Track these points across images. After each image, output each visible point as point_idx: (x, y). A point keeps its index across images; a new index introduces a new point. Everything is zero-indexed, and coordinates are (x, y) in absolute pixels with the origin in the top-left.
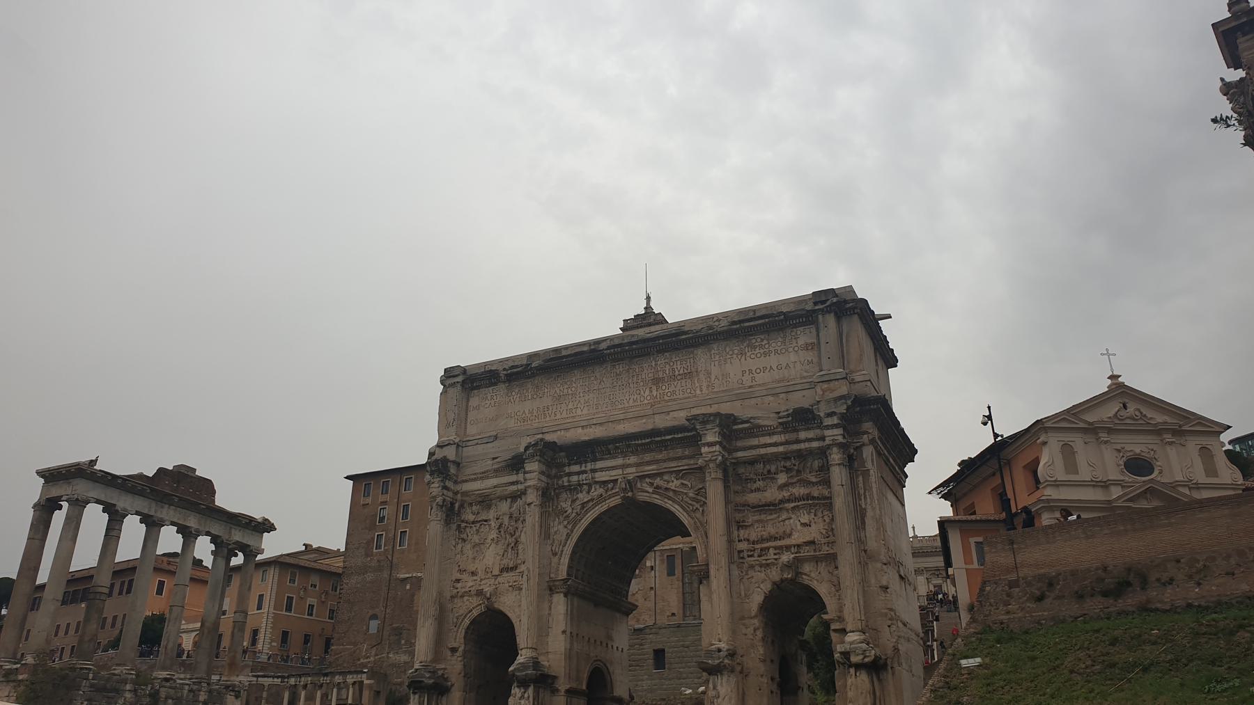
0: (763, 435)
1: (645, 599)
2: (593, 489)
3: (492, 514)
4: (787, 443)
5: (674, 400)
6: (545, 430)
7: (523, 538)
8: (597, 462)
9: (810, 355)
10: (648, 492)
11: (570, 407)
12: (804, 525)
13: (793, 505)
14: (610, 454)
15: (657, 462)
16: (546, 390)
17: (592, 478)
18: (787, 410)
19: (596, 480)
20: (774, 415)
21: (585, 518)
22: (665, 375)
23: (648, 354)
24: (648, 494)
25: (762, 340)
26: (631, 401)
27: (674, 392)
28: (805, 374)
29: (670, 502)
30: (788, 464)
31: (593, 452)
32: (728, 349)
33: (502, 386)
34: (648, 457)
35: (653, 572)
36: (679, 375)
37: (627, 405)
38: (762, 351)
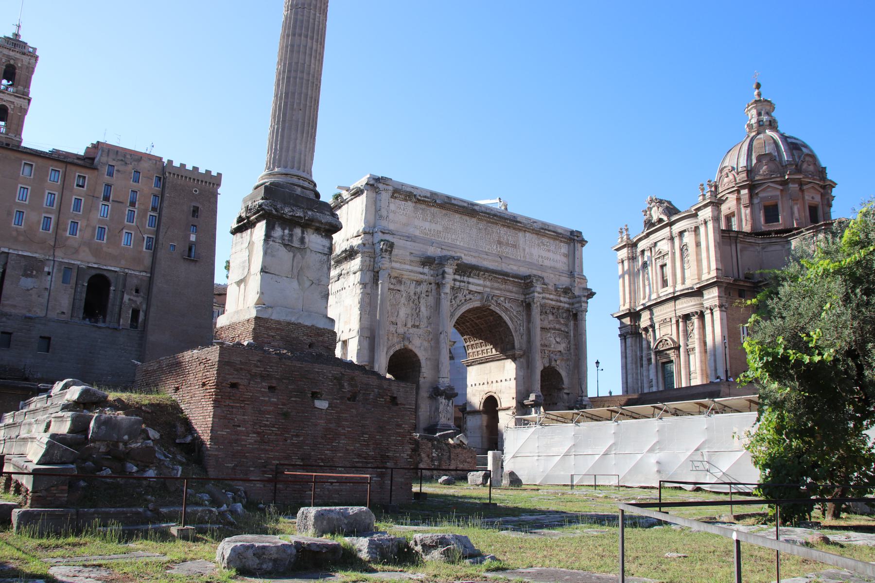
0: (547, 293)
1: (39, 296)
3: (402, 288)
5: (509, 258)
6: (443, 247)
7: (423, 309)
9: (565, 260)
15: (500, 290)
26: (487, 249)
27: (508, 253)
30: (554, 311)
31: (470, 273)
33: (409, 203)
34: (496, 285)
35: (49, 277)
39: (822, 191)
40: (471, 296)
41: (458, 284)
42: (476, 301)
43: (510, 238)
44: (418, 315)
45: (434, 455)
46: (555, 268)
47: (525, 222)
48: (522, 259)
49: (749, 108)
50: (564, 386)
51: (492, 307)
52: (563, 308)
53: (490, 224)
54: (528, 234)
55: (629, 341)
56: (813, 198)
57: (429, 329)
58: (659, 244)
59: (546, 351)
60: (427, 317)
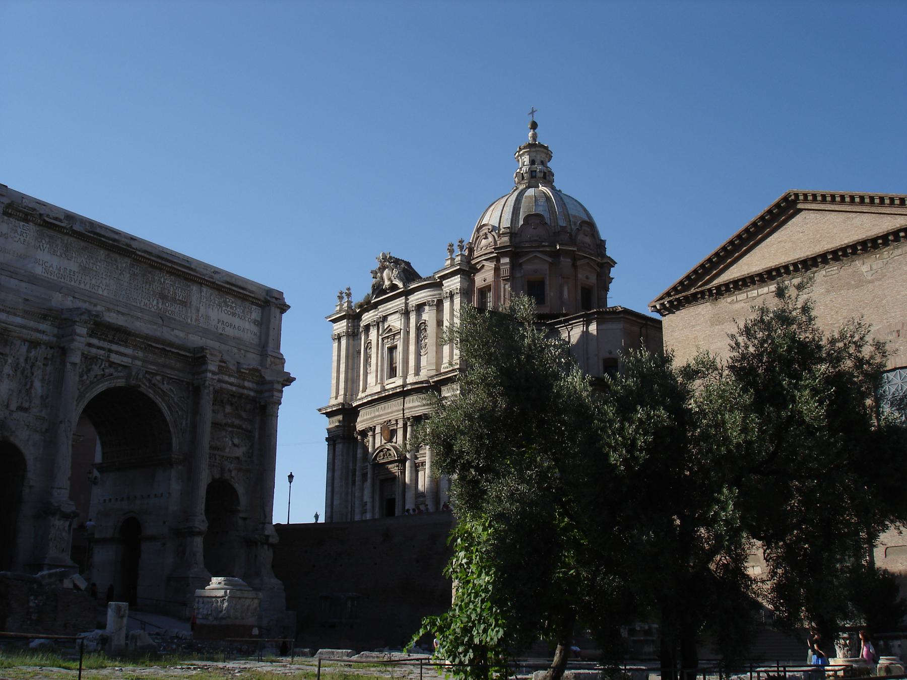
0: (226, 375)
2: (103, 366)
4: (239, 386)
5: (175, 320)
6: (77, 295)
7: (37, 384)
8: (112, 344)
9: (254, 329)
10: (146, 386)
11: (94, 281)
12: (235, 445)
13: (230, 429)
14: (125, 343)
16: (74, 255)
17: (108, 357)
18: (249, 365)
19: (111, 359)
20: (235, 363)
21: (97, 388)
22: (169, 295)
23: (161, 269)
24: (145, 387)
25: (232, 303)
26: (142, 304)
28: (252, 341)
29: (160, 399)
32: (212, 297)
34: (151, 357)
36: (179, 300)
37: (138, 305)
38: (232, 311)
39: (598, 269)
40: (112, 370)
41: (94, 351)
42: (118, 377)
43: (179, 292)
44: (28, 392)
45: (31, 604)
46: (239, 339)
47: (202, 270)
48: (193, 323)
49: (521, 152)
50: (239, 508)
51: (143, 389)
52: (247, 397)
53: (150, 269)
54: (204, 289)
55: (339, 447)
56: (587, 278)
57: (43, 414)
58: (389, 318)
59: (217, 457)
60: (42, 397)
